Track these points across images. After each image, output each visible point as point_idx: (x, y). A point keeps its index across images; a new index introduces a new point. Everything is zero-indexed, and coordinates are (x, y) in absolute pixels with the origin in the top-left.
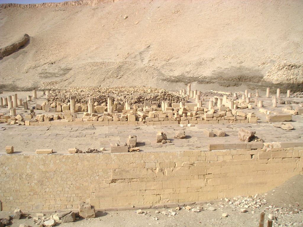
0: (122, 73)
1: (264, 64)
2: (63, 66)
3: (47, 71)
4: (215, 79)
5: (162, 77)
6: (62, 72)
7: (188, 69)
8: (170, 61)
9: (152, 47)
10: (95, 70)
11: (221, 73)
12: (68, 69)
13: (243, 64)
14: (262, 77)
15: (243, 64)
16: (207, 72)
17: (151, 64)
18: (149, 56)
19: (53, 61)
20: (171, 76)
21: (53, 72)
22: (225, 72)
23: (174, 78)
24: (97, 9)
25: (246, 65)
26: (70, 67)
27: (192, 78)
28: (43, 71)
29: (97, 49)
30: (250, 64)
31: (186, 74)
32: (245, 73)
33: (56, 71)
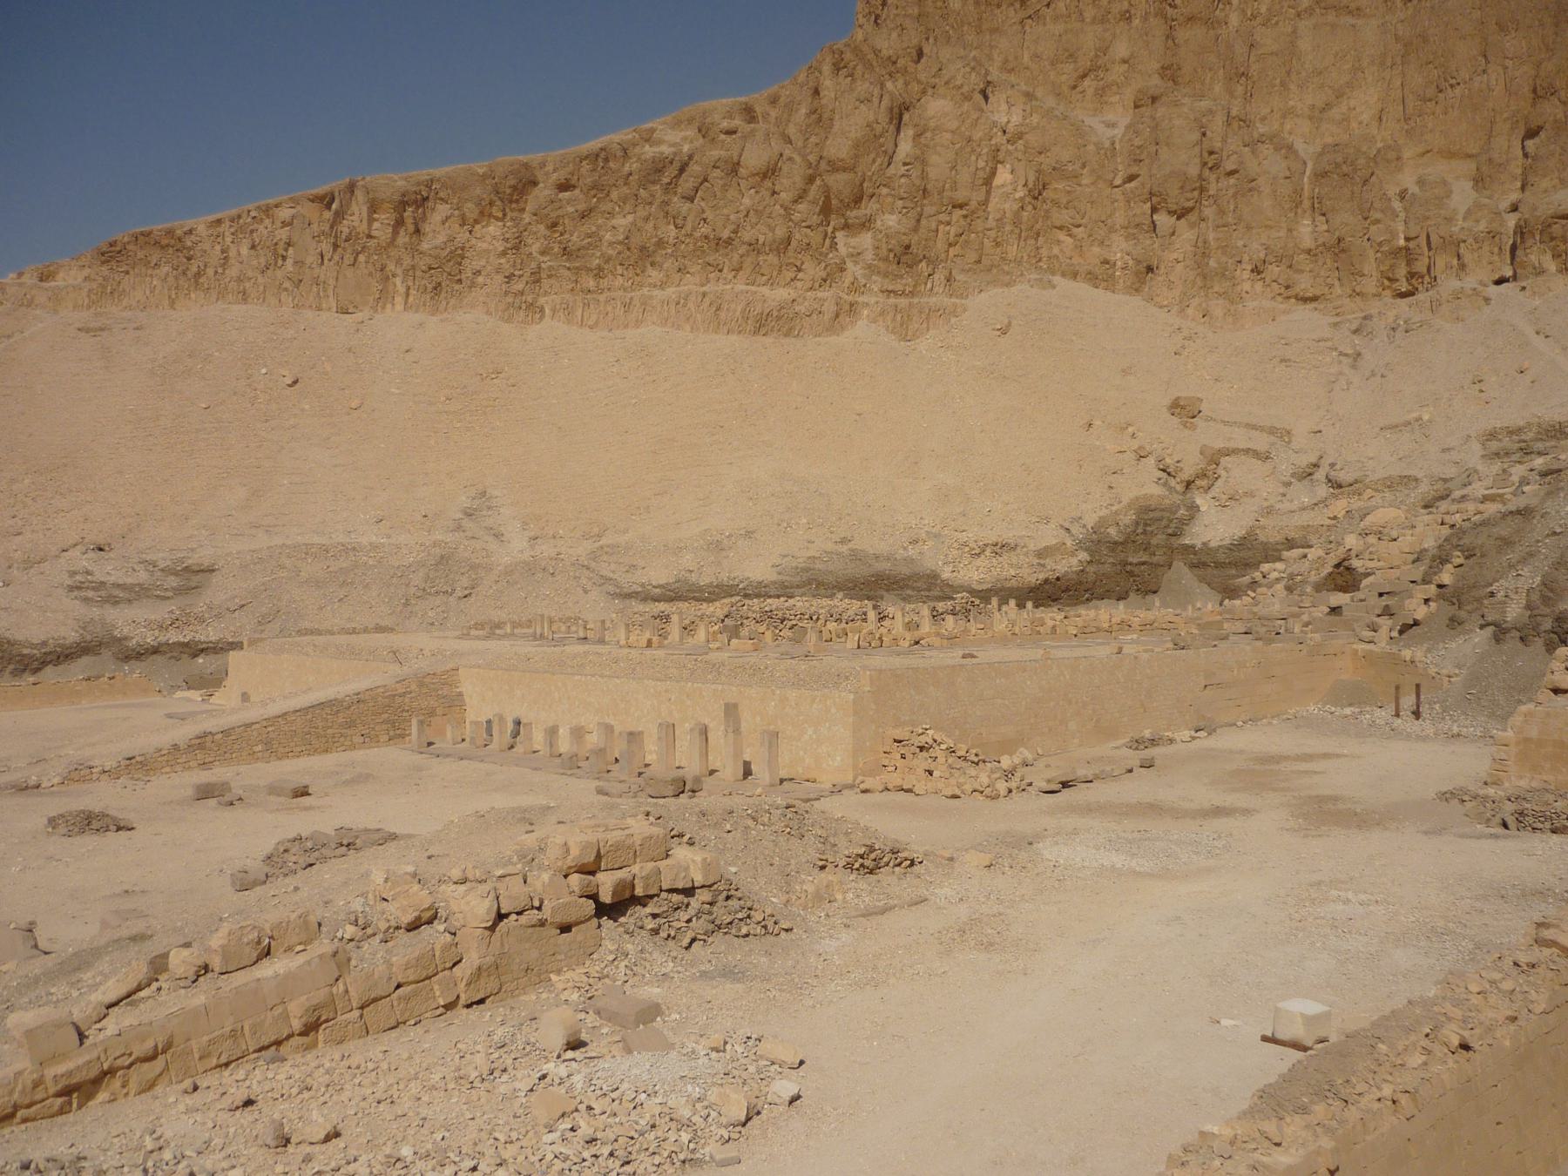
0: (465, 581)
2: (163, 558)
4: (798, 587)
5: (611, 589)
6: (173, 581)
7: (688, 560)
9: (496, 493)
11: (807, 570)
15: (850, 545)
16: (758, 568)
19: (101, 541)
20: (643, 585)
21: (129, 581)
22: (819, 566)
24: (102, 329)
28: (78, 578)
30: (881, 543)
31: (693, 578)
33: (142, 576)
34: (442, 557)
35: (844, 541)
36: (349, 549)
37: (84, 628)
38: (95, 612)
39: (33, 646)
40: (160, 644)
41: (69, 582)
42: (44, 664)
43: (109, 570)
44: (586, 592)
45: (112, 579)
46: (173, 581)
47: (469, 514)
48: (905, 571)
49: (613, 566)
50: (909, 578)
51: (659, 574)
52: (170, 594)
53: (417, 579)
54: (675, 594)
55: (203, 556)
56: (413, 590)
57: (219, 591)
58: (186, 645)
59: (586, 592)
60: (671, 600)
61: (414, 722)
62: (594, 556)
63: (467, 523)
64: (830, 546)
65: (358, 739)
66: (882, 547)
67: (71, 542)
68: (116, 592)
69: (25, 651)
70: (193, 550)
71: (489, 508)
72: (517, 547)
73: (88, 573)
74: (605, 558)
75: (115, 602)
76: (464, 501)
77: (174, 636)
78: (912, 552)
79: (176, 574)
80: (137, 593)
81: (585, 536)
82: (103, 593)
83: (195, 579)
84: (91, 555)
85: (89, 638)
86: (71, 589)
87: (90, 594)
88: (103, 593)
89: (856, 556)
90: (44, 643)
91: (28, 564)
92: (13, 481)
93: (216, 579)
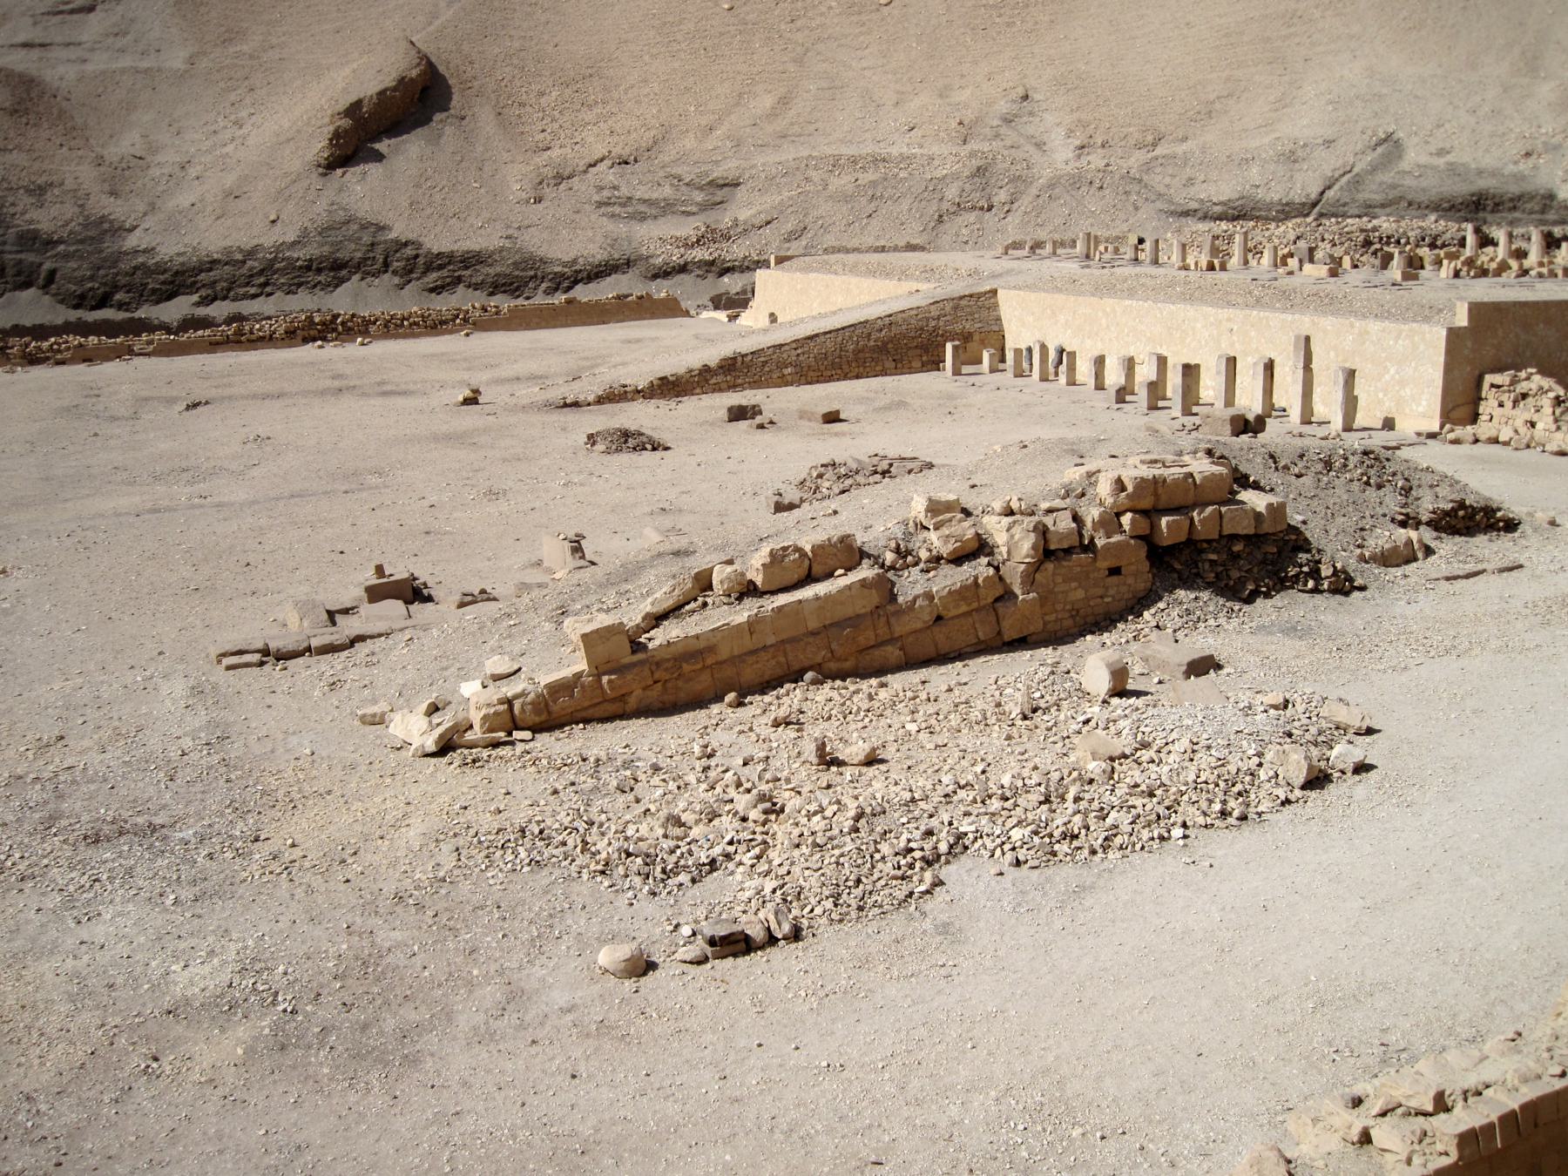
1: (1528, 155)
3: (625, 191)
4: (1383, 206)
5: (1165, 207)
6: (699, 197)
8: (1159, 151)
10: (873, 184)
11: (1394, 187)
12: (721, 182)
13: (1450, 158)
14: (1551, 196)
15: (1450, 158)
17: (1096, 160)
18: (1062, 131)
21: (655, 196)
23: (1218, 209)
25: (1463, 156)
26: (717, 173)
27: (1287, 204)
28: (606, 193)
29: (784, 102)
31: (1261, 194)
32: (1483, 184)
33: (667, 191)
34: (979, 169)
35: (1441, 152)
36: (878, 160)
37: (612, 246)
38: (622, 228)
39: (565, 265)
40: (686, 264)
41: (596, 198)
42: (576, 282)
43: (637, 185)
44: (1137, 209)
45: (638, 195)
46: (699, 197)
47: (1008, 120)
48: (1514, 189)
49: (1167, 180)
50: (1520, 197)
51: (1224, 190)
52: (695, 209)
53: (952, 192)
54: (1238, 213)
55: (727, 168)
56: (945, 205)
57: (743, 209)
58: (712, 263)
59: (1137, 209)
60: (1235, 218)
61: (949, 346)
62: (1147, 167)
63: (1003, 130)
64: (1424, 159)
65: (890, 364)
66: (1488, 161)
67: (599, 156)
68: (642, 208)
69: (558, 269)
70: (717, 162)
71: (1031, 114)
72: (1062, 156)
73: (615, 188)
74: (1159, 170)
75: (643, 218)
76: (1003, 107)
77: (700, 254)
78: (1524, 166)
79: (701, 188)
80: (666, 208)
81: (1139, 146)
82: (630, 209)
83: (720, 194)
84: (617, 169)
85: (616, 256)
86: (600, 204)
87: (617, 209)
88: (630, 209)
89: (1452, 169)
90: (575, 261)
91: (560, 178)
92: (542, 94)
93: (741, 193)
